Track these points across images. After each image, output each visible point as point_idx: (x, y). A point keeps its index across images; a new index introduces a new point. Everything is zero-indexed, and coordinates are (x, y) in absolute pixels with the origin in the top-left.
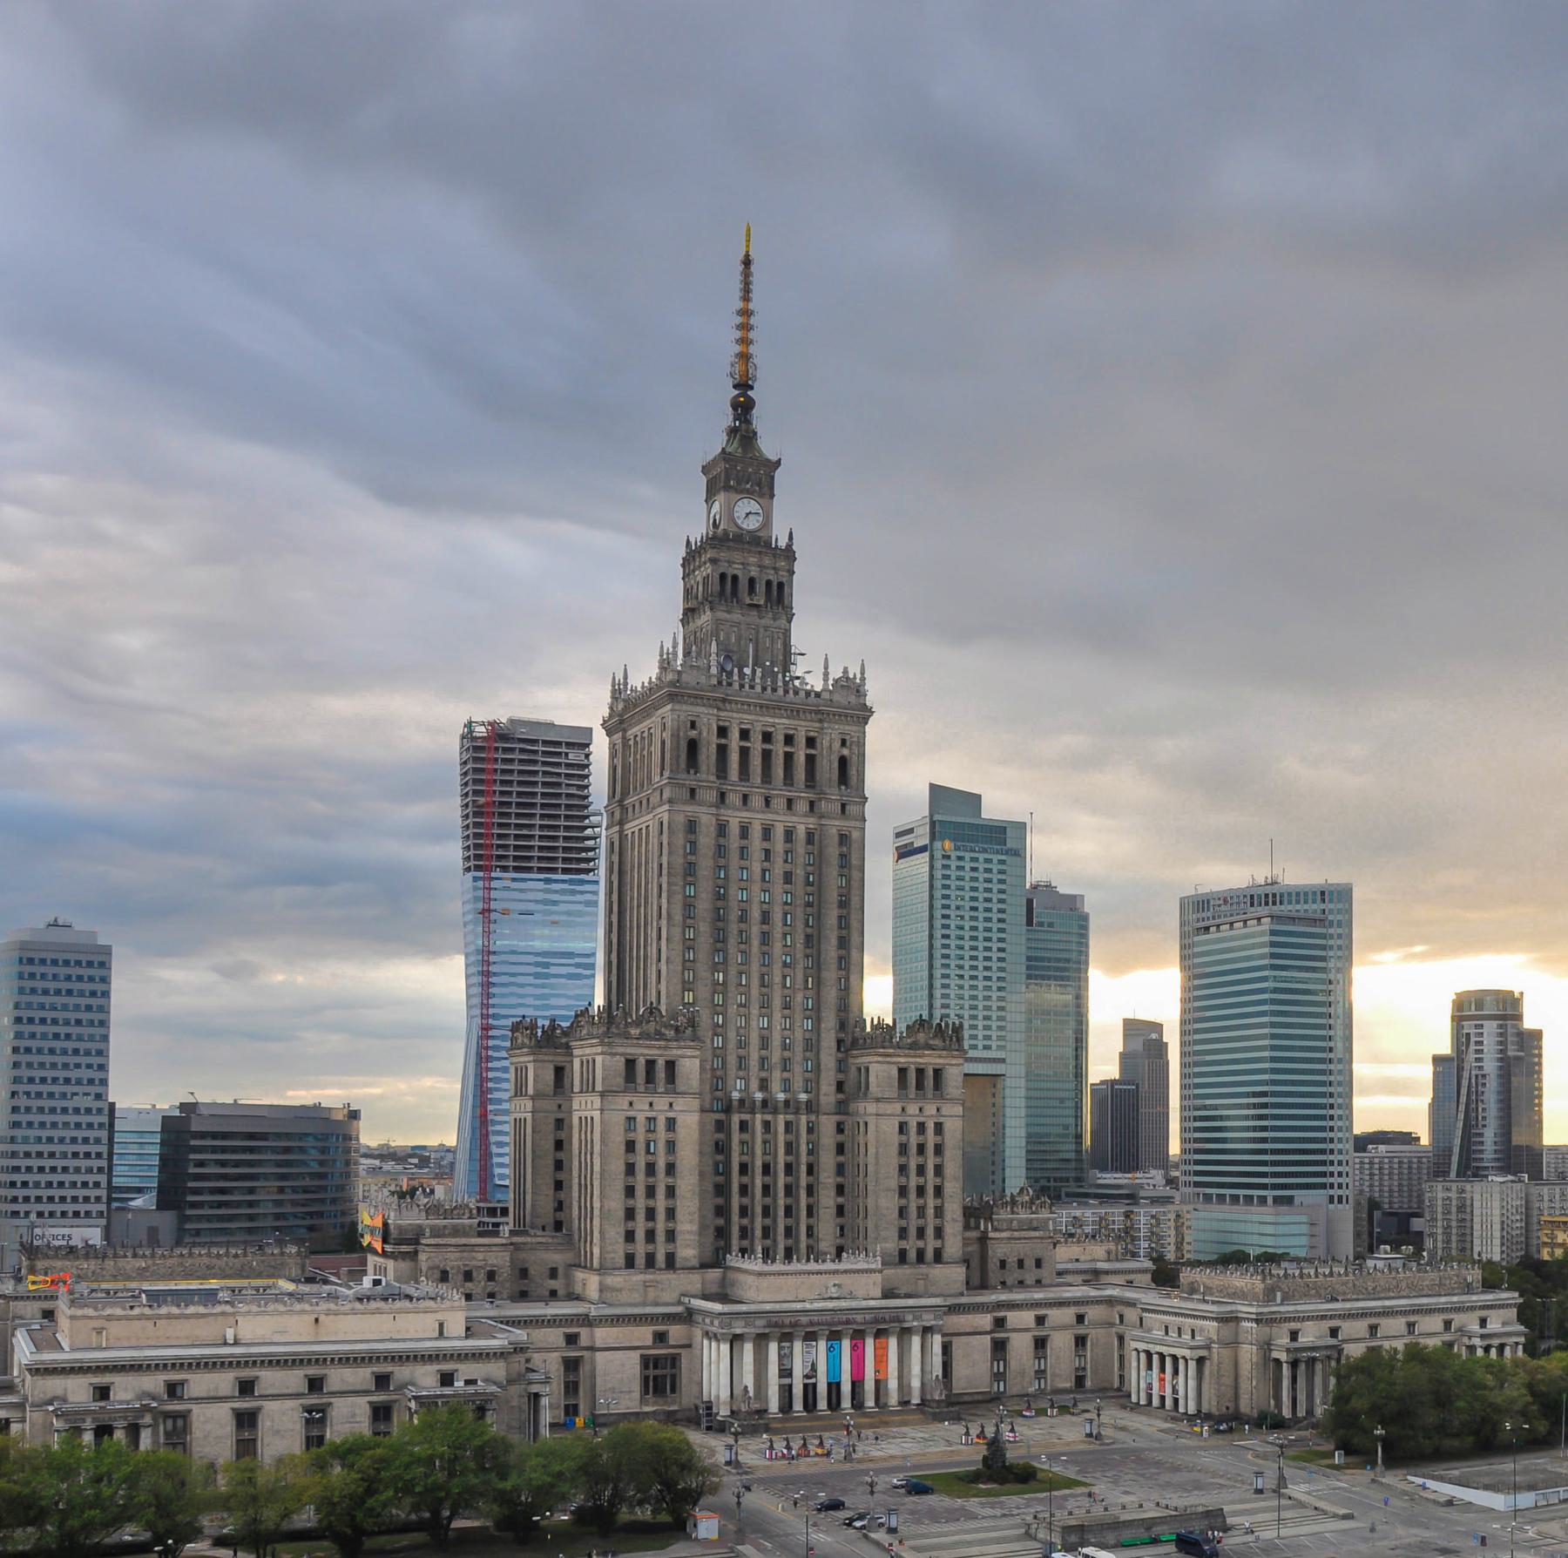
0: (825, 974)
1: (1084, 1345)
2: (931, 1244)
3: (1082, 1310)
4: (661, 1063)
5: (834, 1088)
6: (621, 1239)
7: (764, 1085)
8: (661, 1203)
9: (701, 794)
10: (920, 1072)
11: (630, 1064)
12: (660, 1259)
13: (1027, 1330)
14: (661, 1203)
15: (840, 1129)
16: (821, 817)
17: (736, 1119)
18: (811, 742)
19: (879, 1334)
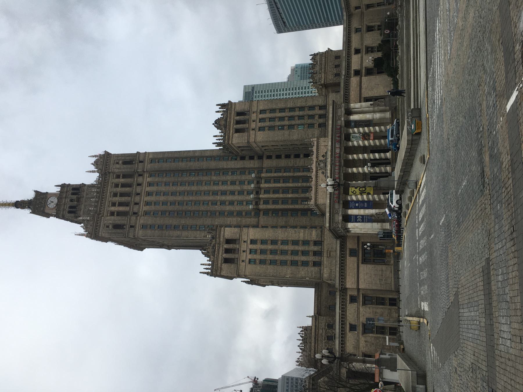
0: (204, 167)
2: (317, 111)
3: (353, 30)
4: (226, 246)
5: (252, 161)
6: (306, 268)
7: (249, 193)
8: (290, 247)
9: (132, 224)
10: (238, 122)
11: (227, 261)
12: (316, 248)
13: (362, 58)
14: (290, 247)
15: (269, 157)
16: (144, 172)
17: (262, 206)
18: (118, 177)
19: (348, 138)
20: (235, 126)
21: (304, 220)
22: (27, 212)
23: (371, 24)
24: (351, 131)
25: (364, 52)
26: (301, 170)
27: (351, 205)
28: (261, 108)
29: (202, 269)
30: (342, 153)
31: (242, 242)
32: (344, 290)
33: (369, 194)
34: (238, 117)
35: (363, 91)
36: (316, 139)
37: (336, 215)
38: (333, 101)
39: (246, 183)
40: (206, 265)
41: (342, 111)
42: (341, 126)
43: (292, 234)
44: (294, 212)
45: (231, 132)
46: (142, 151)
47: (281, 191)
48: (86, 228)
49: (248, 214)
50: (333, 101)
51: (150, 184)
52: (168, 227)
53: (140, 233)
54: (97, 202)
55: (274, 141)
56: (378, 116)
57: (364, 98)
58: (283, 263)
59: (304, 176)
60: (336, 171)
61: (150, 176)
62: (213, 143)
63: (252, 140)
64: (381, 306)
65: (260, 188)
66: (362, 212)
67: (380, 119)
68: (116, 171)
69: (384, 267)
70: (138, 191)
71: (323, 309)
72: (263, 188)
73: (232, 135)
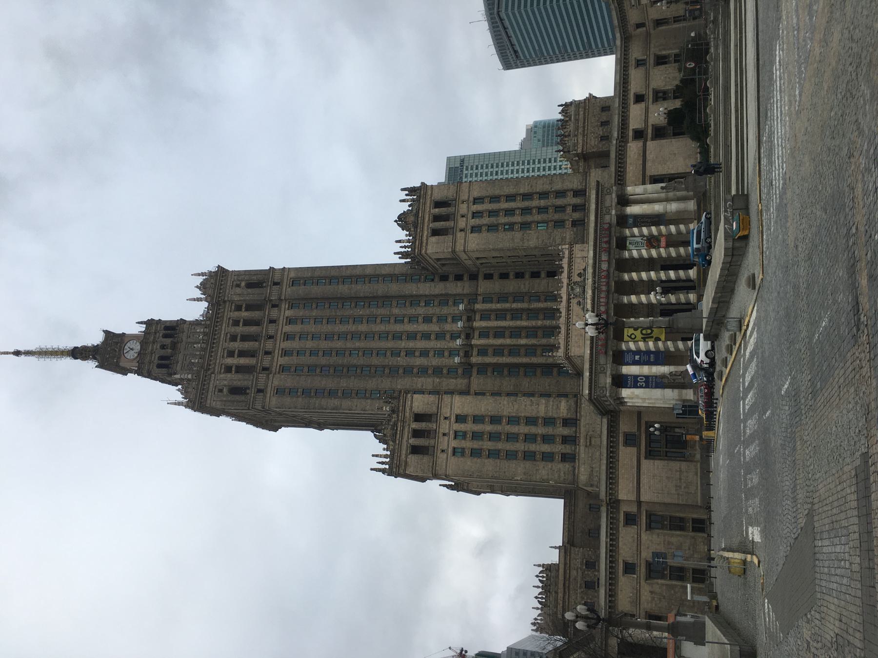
0: (380, 293)
1: (665, 57)
2: (570, 200)
3: (632, 62)
5: (459, 284)
6: (550, 465)
7: (454, 336)
8: (523, 429)
9: (261, 386)
10: (437, 218)
11: (415, 450)
12: (566, 431)
13: (647, 110)
14: (523, 429)
15: (488, 277)
16: (280, 300)
17: (474, 360)
18: (239, 308)
19: (622, 244)
20: (431, 225)
21: (545, 383)
22: (90, 365)
23: (664, 53)
24: (627, 232)
25: (651, 100)
26: (542, 298)
27: (628, 358)
28: (476, 194)
29: (374, 463)
30: (612, 270)
31: (442, 418)
32: (614, 503)
33: (658, 339)
34: (437, 210)
35: (649, 164)
36: (567, 246)
37: (602, 376)
38: (598, 182)
39: (449, 320)
40: (381, 456)
41: (612, 200)
42: (610, 224)
43: (525, 407)
44: (530, 369)
45: (425, 234)
46: (278, 266)
47: (507, 333)
48: (185, 392)
49: (452, 371)
50: (598, 182)
51: (290, 321)
52: (318, 393)
53: (273, 402)
54: (204, 350)
55: (497, 250)
56: (673, 207)
57: (650, 176)
58: (511, 455)
59: (546, 309)
60: (602, 300)
61: (291, 307)
62: (395, 253)
63: (459, 247)
64: (678, 533)
65: (473, 329)
66: (646, 370)
67: (678, 212)
68: (236, 298)
69: (684, 465)
70: (271, 332)
71: (578, 535)
72: (477, 328)
73: (427, 240)
